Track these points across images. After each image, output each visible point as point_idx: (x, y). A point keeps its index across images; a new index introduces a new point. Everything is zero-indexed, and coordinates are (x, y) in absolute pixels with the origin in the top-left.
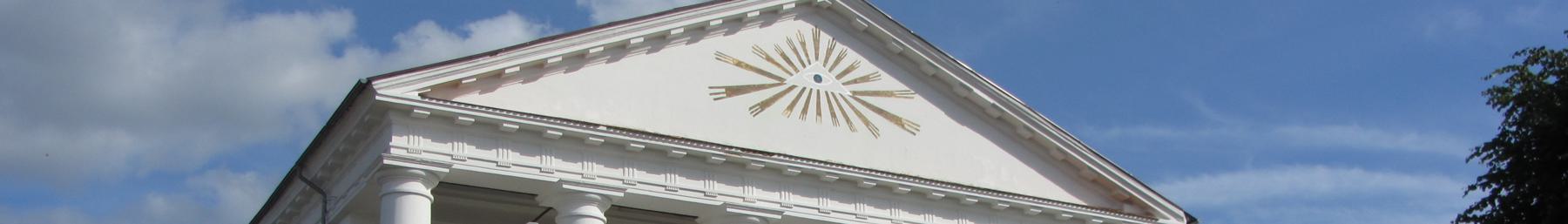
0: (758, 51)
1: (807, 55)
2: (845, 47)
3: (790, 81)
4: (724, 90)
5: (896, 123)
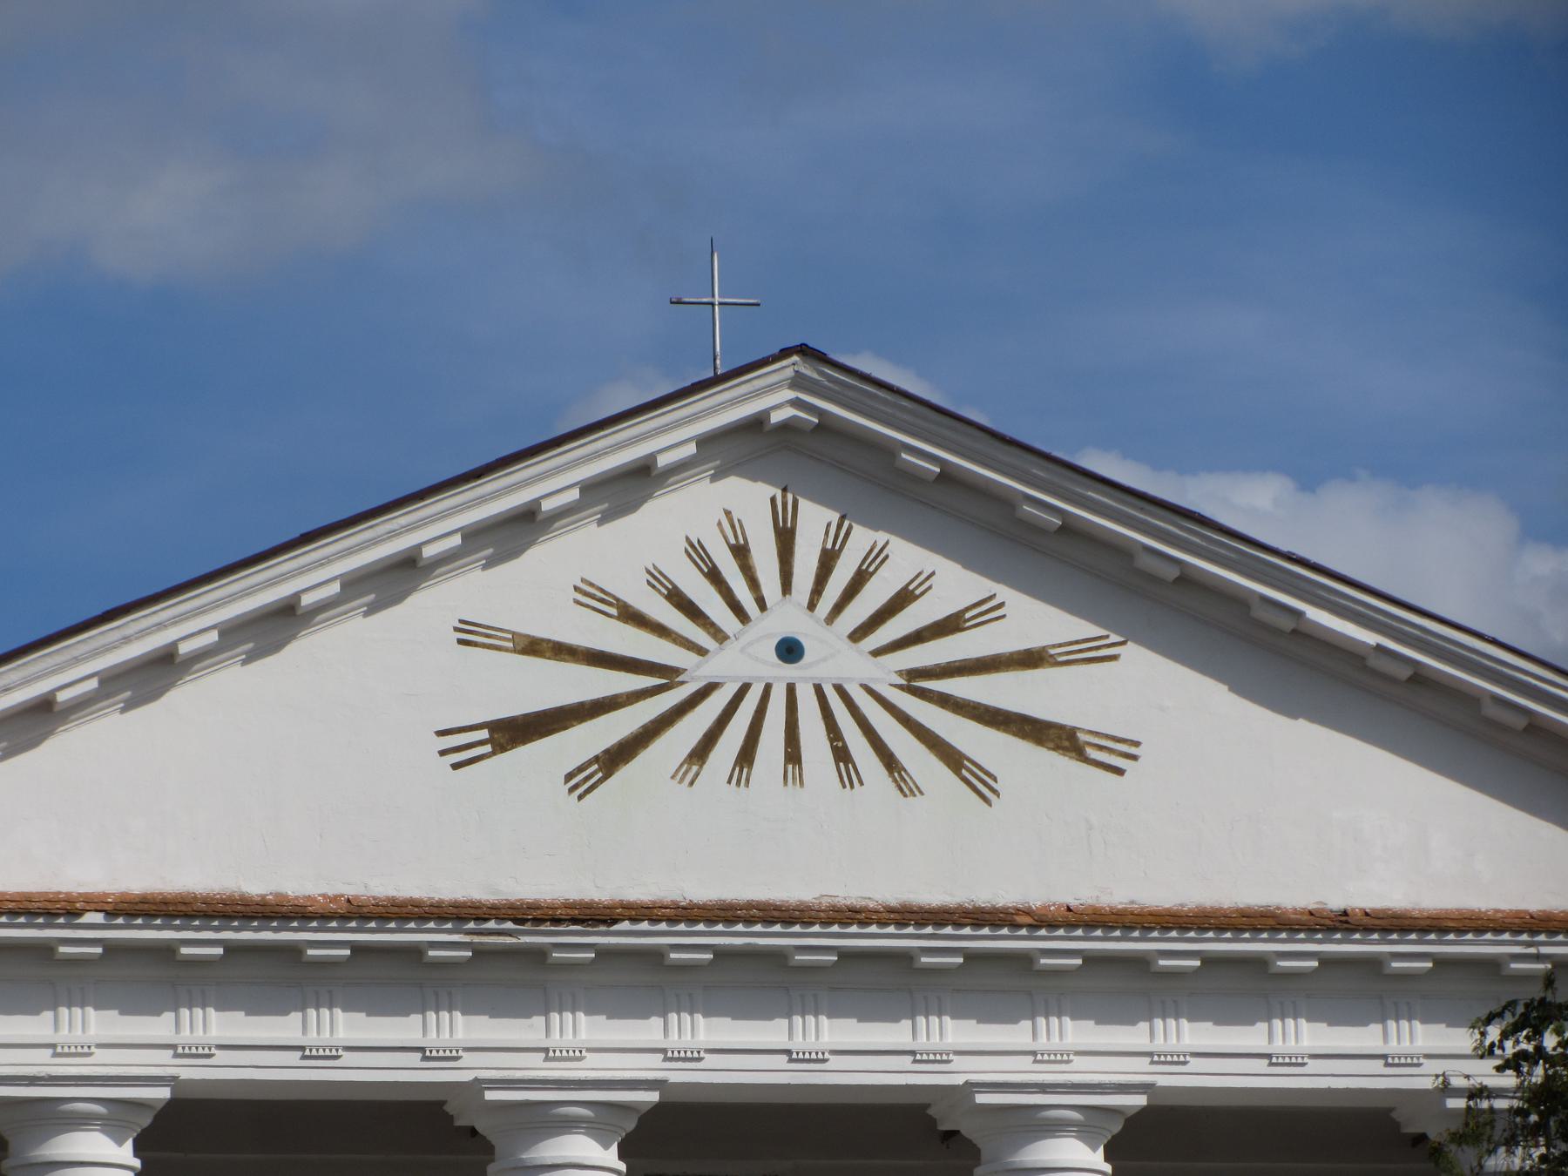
0: (593, 596)
1: (753, 583)
2: (881, 537)
4: (484, 734)
5: (1057, 748)
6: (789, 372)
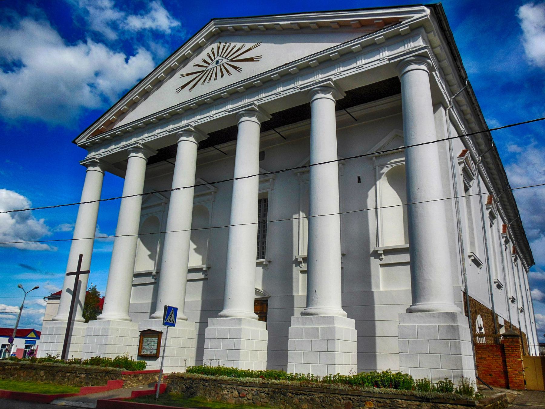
3: (207, 69)
6: (213, 23)
